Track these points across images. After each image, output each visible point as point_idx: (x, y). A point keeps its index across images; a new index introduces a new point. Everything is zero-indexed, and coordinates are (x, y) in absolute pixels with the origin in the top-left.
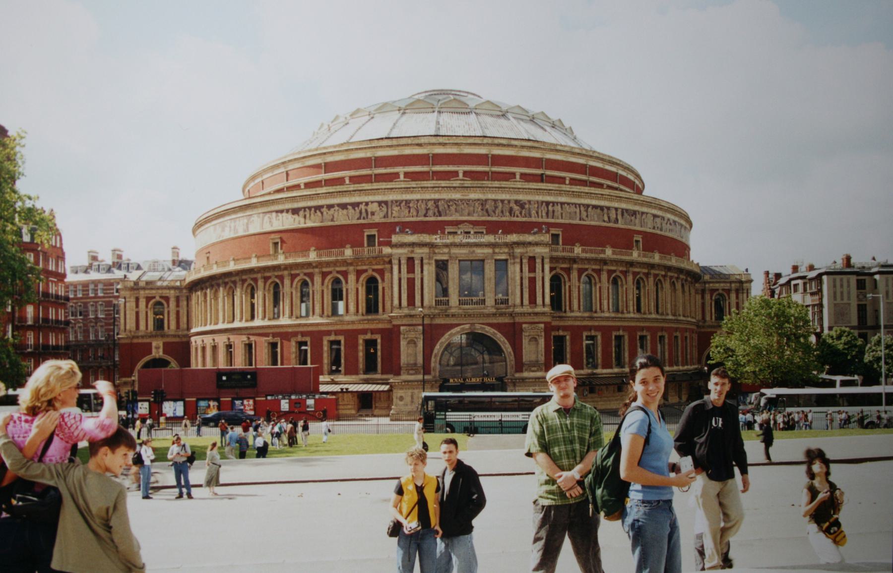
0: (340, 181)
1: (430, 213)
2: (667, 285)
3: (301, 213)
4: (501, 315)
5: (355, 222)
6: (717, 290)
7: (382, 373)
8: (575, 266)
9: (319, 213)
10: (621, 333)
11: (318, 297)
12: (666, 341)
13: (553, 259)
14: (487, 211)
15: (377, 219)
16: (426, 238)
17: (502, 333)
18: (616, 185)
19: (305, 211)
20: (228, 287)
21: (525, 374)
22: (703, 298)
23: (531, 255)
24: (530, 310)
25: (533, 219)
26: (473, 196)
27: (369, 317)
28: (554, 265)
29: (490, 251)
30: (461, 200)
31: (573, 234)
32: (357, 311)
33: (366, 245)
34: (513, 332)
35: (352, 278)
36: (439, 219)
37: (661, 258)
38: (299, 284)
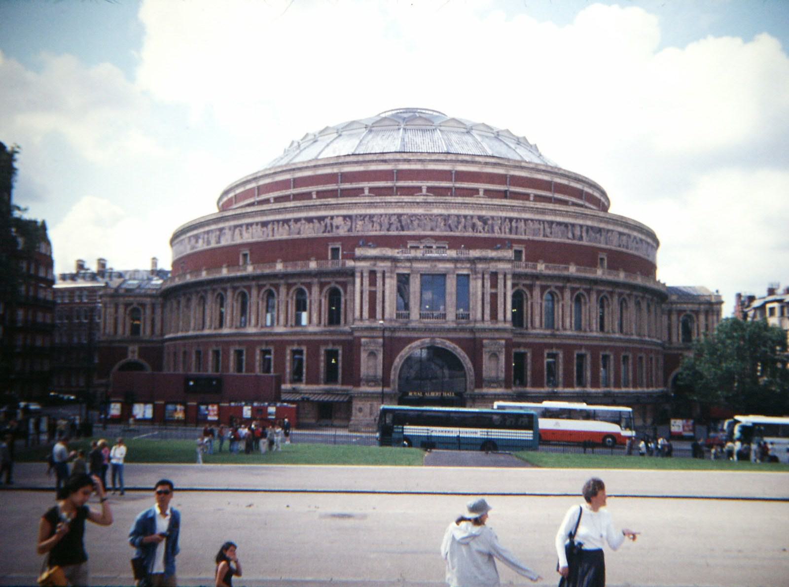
0: (308, 196)
1: (393, 227)
2: (632, 304)
3: (270, 226)
4: (463, 330)
5: (321, 235)
6: (685, 311)
7: (343, 384)
8: (538, 283)
9: (286, 226)
10: (583, 351)
11: (282, 308)
12: (630, 361)
13: (515, 276)
14: (450, 226)
15: (342, 232)
16: (389, 252)
17: (462, 348)
18: (581, 202)
19: (273, 224)
20: (199, 295)
21: (485, 390)
22: (669, 319)
23: (494, 270)
24: (491, 326)
25: (496, 235)
26: (436, 211)
27: (332, 328)
28: (516, 282)
29: (450, 266)
30: (424, 215)
31: (537, 250)
32: (320, 322)
33: (330, 258)
34: (474, 347)
35: (315, 290)
36: (402, 233)
37: (626, 277)
38: (265, 296)
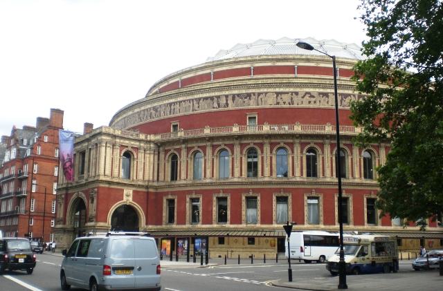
8: (183, 146)
25: (162, 118)
31: (190, 122)
